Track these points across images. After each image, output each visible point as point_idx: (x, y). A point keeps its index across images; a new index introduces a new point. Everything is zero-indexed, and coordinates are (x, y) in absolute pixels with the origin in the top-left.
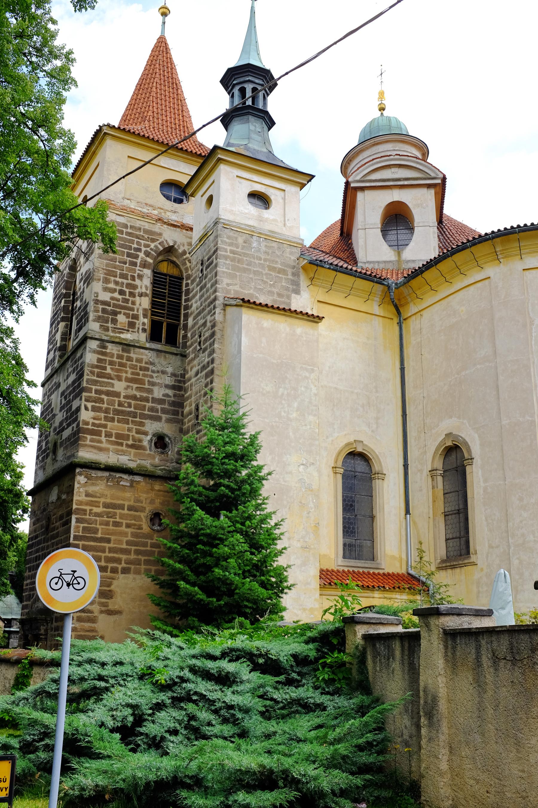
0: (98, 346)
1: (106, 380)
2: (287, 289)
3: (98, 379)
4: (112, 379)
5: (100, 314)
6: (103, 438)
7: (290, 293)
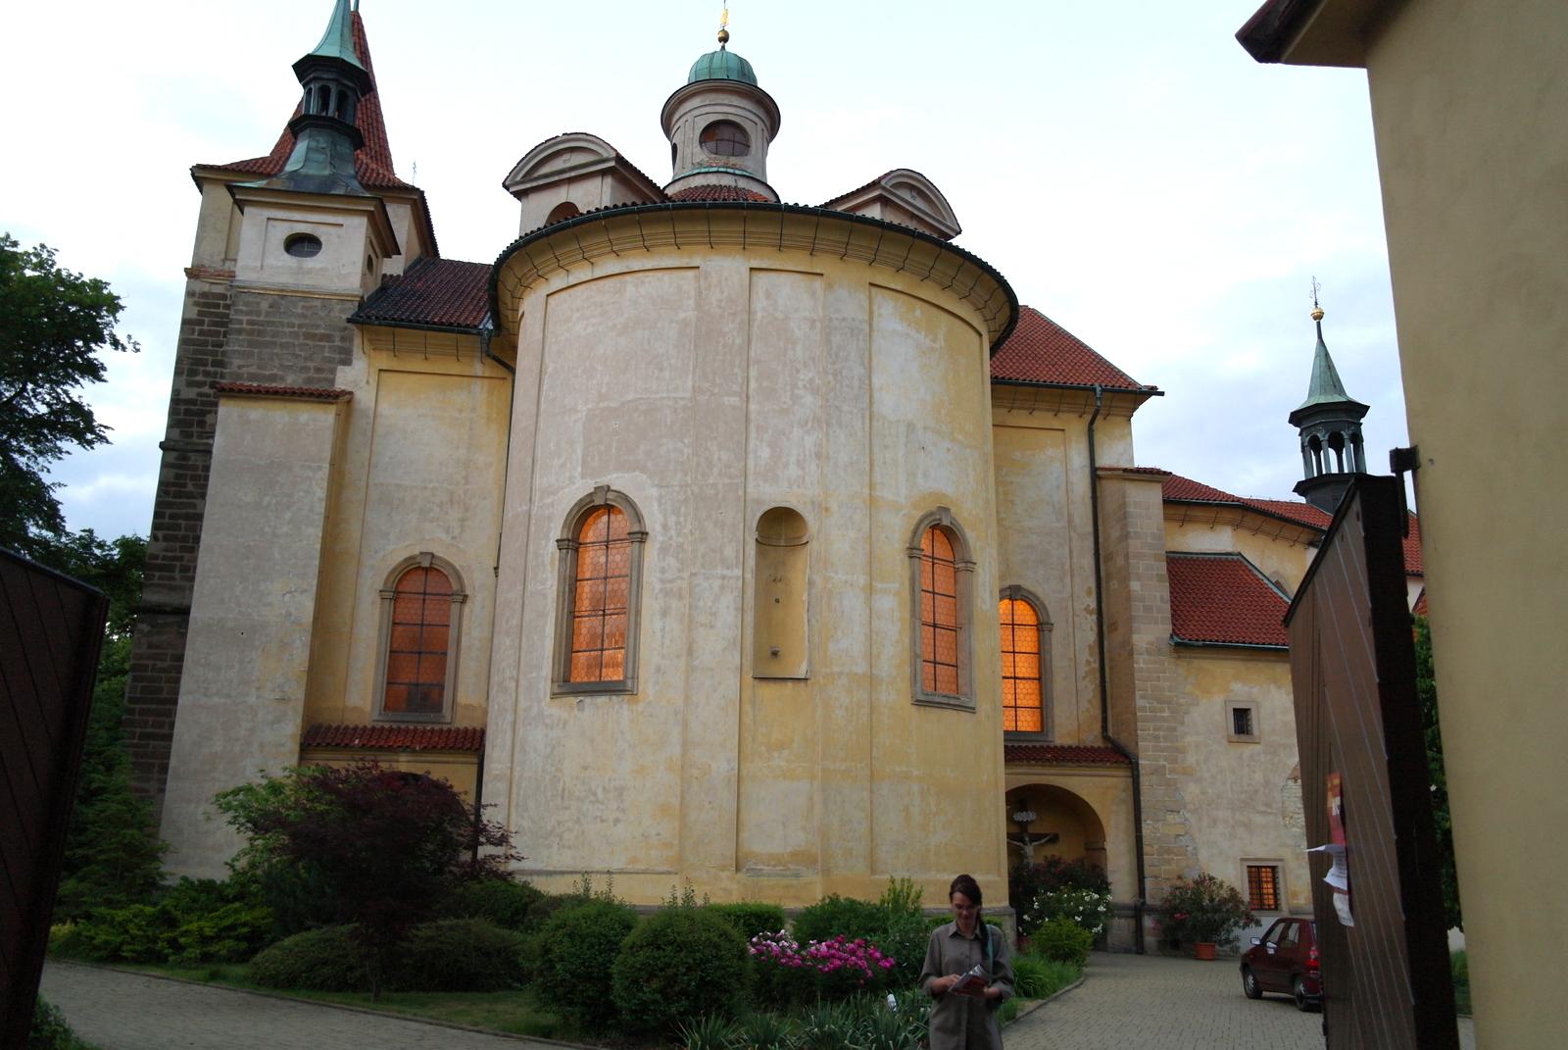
0: (176, 459)
1: (185, 500)
2: (330, 360)
3: (174, 500)
4: (194, 498)
5: (182, 417)
6: (177, 575)
7: (333, 366)
